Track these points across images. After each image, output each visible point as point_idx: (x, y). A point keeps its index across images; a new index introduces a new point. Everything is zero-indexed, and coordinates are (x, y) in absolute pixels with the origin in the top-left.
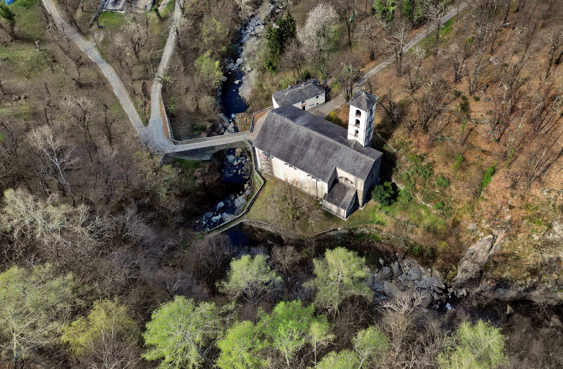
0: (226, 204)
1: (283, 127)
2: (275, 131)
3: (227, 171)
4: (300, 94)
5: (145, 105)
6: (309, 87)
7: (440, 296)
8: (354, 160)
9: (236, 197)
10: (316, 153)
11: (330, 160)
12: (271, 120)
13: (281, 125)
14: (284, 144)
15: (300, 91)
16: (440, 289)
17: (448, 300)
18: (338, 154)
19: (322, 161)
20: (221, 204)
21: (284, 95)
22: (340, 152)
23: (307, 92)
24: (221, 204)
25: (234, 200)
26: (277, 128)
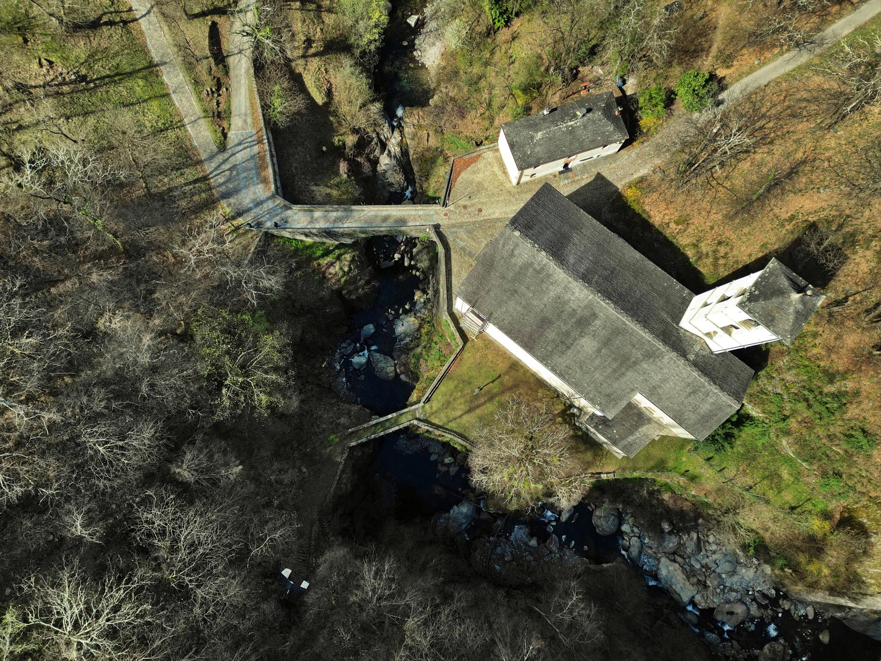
0: (378, 327)
1: (531, 270)
2: (511, 275)
3: (384, 253)
4: (569, 137)
5: (218, 90)
6: (594, 122)
7: (762, 610)
8: (688, 390)
9: (397, 316)
10: (599, 350)
11: (630, 374)
12: (507, 247)
13: (528, 265)
14: (527, 307)
15: (572, 131)
16: (765, 596)
17: (774, 619)
18: (653, 367)
19: (610, 370)
20: (370, 328)
21: (532, 138)
22: (659, 364)
23: (586, 136)
24: (370, 328)
25: (393, 320)
26: (517, 269)
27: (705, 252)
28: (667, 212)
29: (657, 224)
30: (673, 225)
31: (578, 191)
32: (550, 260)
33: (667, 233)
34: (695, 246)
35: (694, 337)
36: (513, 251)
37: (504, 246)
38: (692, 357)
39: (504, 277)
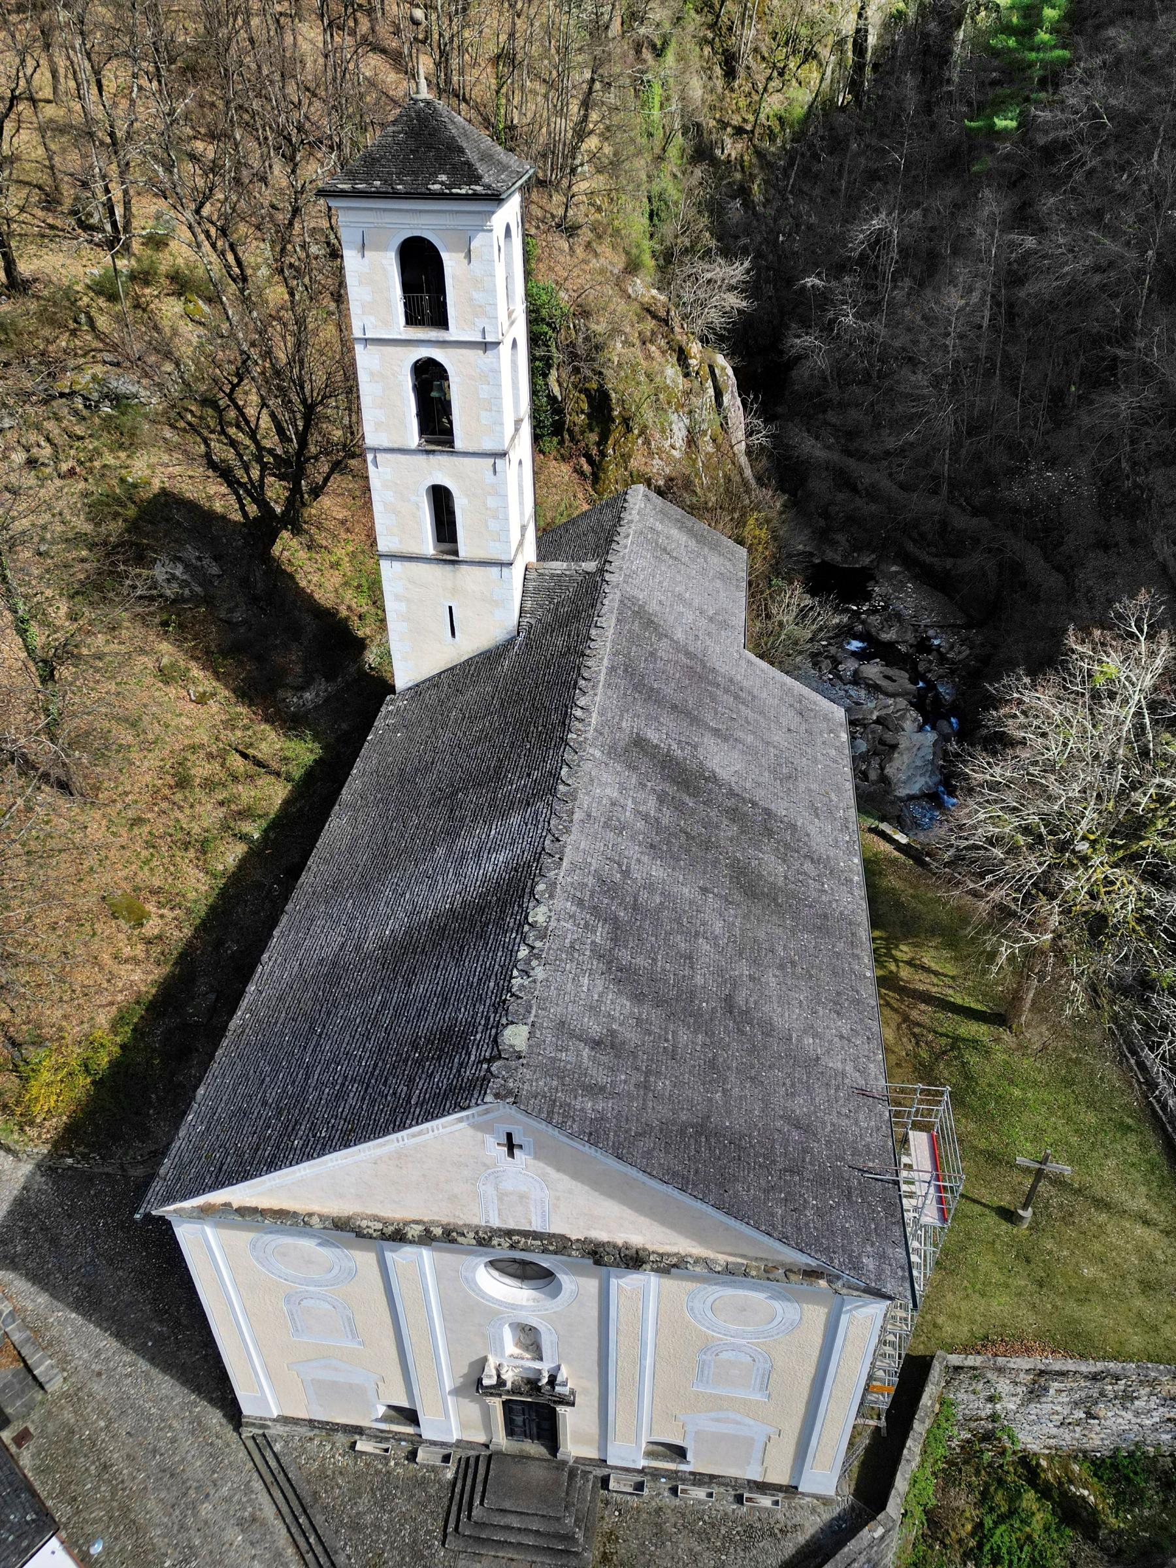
27: (221, 812)
28: (106, 958)
29: (158, 973)
30: (152, 927)
31: (77, 1305)
32: (553, 885)
33: (180, 935)
34: (204, 847)
35: (531, 585)
36: (596, 1044)
37: (595, 1090)
38: (591, 566)
39: (712, 1064)
